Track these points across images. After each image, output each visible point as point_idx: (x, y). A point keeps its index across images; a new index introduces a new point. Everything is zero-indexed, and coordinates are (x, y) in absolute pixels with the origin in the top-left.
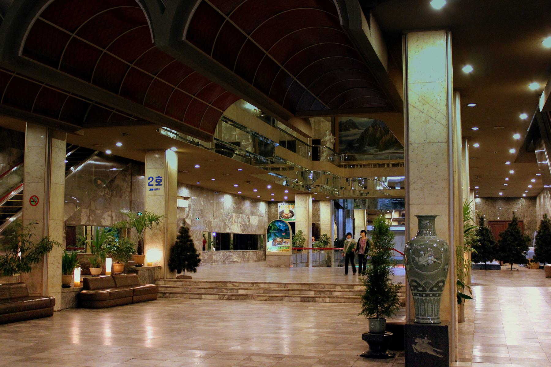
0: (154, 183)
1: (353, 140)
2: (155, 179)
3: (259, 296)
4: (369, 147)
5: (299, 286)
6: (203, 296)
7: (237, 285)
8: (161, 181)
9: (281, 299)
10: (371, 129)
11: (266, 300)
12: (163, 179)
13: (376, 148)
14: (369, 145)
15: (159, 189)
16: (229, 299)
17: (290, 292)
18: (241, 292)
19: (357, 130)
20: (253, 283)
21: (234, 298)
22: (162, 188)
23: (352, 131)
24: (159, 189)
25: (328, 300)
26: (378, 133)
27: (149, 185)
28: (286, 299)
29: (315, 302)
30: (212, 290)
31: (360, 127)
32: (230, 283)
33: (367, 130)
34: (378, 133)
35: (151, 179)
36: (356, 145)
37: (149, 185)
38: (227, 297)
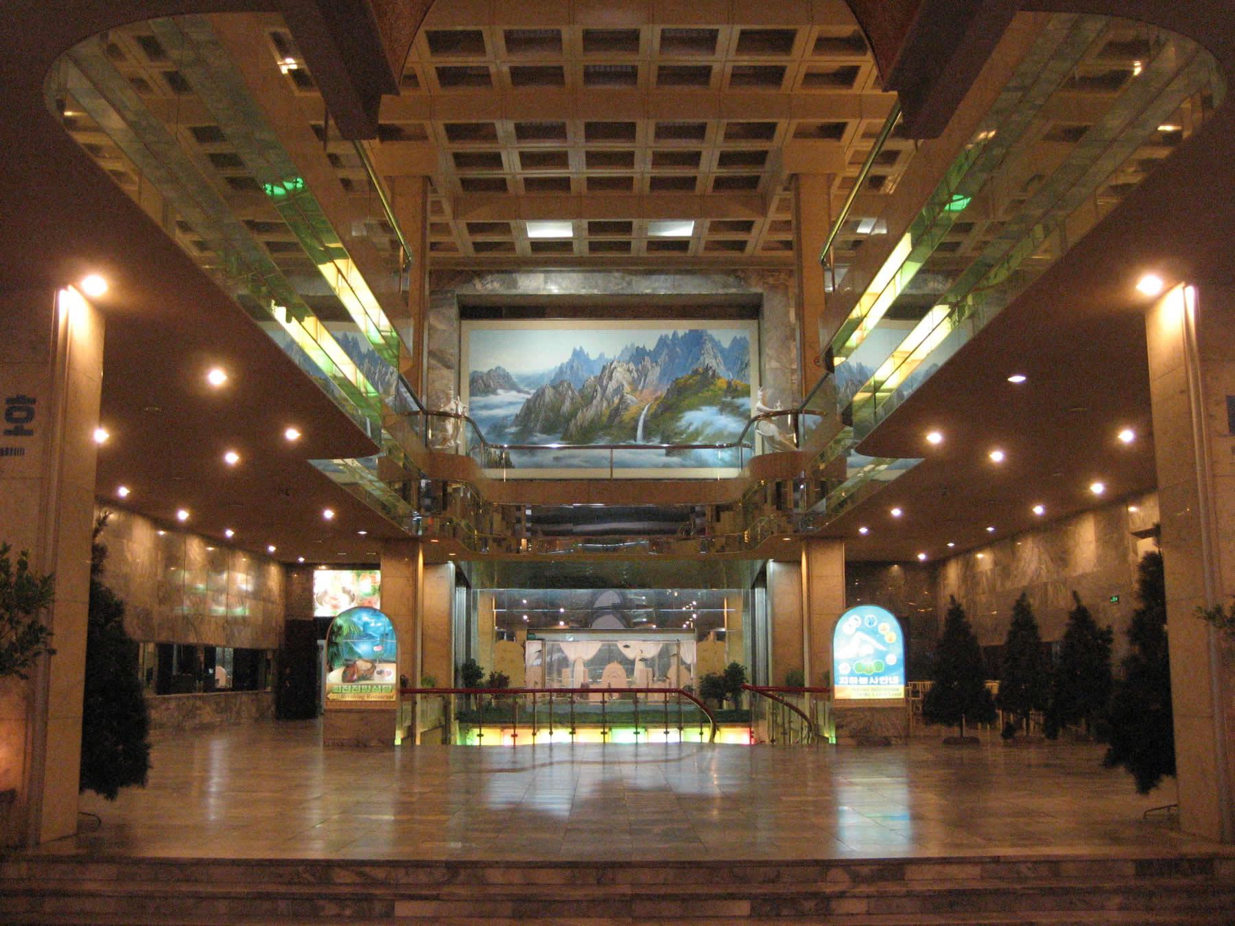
1: (506, 418)
4: (544, 436)
10: (549, 393)
13: (562, 439)
19: (514, 393)
23: (503, 396)
31: (522, 387)
33: (540, 394)
36: (513, 430)
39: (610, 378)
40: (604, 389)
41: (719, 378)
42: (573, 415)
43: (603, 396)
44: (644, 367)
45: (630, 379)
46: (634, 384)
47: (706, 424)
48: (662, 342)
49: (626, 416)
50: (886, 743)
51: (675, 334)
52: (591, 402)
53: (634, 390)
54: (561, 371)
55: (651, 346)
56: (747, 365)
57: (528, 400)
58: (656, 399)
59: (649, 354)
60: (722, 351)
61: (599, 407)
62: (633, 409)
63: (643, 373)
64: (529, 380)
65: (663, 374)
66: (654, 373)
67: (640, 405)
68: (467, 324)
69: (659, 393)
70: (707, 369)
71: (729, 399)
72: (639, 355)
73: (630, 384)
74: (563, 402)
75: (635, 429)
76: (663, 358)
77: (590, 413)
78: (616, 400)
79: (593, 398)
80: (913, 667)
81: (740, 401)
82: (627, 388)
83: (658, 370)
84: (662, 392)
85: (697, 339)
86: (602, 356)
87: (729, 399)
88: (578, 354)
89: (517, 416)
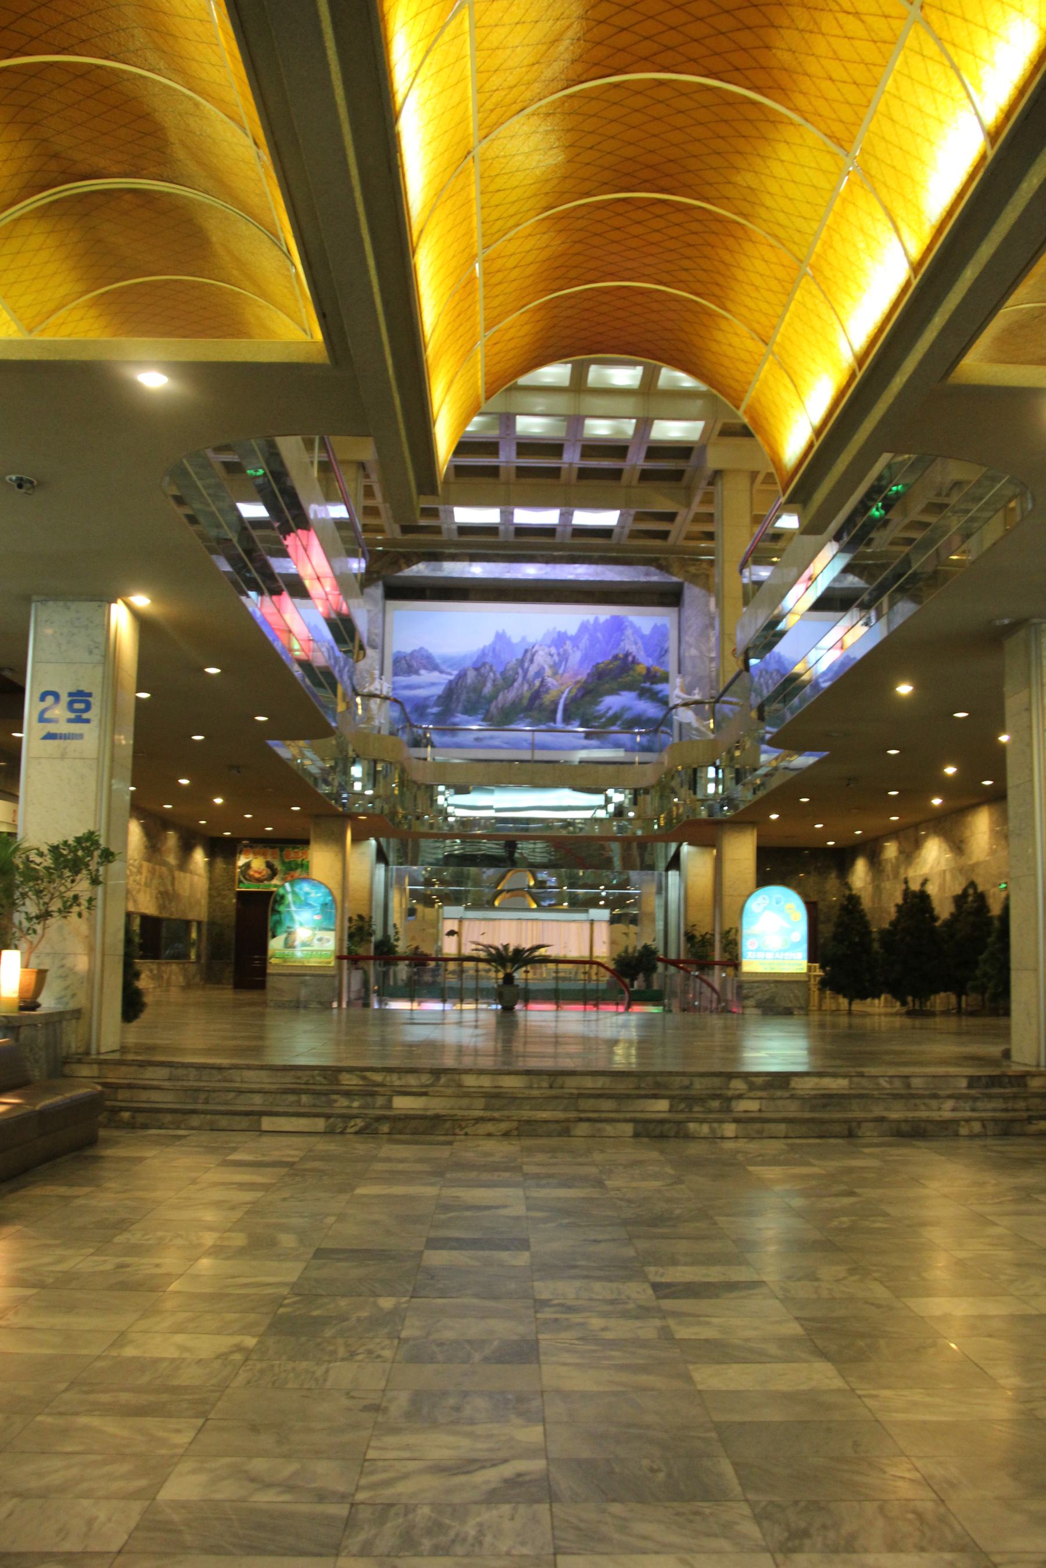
0: (60, 712)
1: (427, 698)
2: (65, 699)
4: (465, 717)
5: (600, 1082)
6: (267, 1123)
7: (378, 1078)
8: (88, 708)
10: (471, 675)
11: (506, 1135)
12: (95, 701)
13: (483, 720)
14: (466, 711)
15: (80, 736)
16: (368, 1131)
17: (583, 1104)
18: (402, 1104)
19: (436, 674)
21: (385, 1128)
23: (426, 676)
24: (80, 736)
26: (489, 685)
27: (42, 719)
28: (583, 1129)
29: (688, 1137)
30: (292, 1098)
31: (444, 667)
32: (351, 1070)
33: (462, 676)
34: (489, 685)
35: (50, 699)
36: (435, 710)
37: (42, 719)
38: (360, 1123)
39: (532, 661)
40: (526, 672)
41: (638, 664)
42: (496, 698)
43: (525, 677)
44: (565, 651)
45: (552, 663)
46: (555, 667)
47: (625, 709)
48: (584, 627)
49: (547, 699)
50: (788, 1012)
51: (596, 620)
52: (512, 685)
53: (555, 674)
54: (483, 653)
56: (666, 651)
57: (450, 682)
58: (577, 683)
59: (571, 638)
60: (642, 637)
61: (520, 690)
63: (564, 657)
65: (585, 658)
66: (575, 657)
67: (561, 688)
68: (391, 604)
69: (579, 678)
71: (648, 685)
72: (560, 639)
73: (551, 667)
74: (484, 685)
75: (554, 711)
76: (584, 642)
77: (511, 695)
78: (537, 683)
79: (514, 680)
81: (658, 687)
82: (548, 672)
84: (582, 677)
85: (617, 626)
86: (524, 639)
87: (648, 685)
88: (500, 637)
89: (439, 697)
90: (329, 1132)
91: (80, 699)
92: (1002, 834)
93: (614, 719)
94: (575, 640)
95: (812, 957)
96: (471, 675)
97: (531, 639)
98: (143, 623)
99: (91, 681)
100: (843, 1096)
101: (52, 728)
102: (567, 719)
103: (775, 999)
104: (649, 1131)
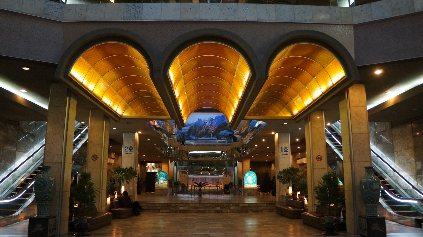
0: (128, 150)
2: (129, 148)
3: (192, 210)
6: (161, 211)
9: (204, 212)
10: (193, 127)
11: (196, 212)
18: (181, 208)
20: (186, 204)
22: (133, 153)
25: (229, 211)
27: (125, 151)
28: (207, 211)
32: (173, 204)
33: (192, 128)
37: (125, 151)
40: (205, 127)
46: (211, 125)
47: (225, 134)
48: (216, 117)
49: (209, 132)
50: (253, 195)
53: (211, 127)
54: (196, 123)
55: (214, 118)
59: (214, 119)
61: (204, 130)
62: (210, 131)
63: (212, 123)
64: (189, 125)
67: (212, 130)
70: (225, 123)
72: (212, 120)
77: (202, 131)
80: (258, 182)
82: (209, 127)
83: (215, 123)
84: (216, 127)
88: (199, 120)
90: (170, 212)
91: (131, 148)
92: (275, 166)
93: (223, 136)
94: (215, 120)
95: (257, 184)
96: (193, 127)
97: (206, 120)
98: (139, 135)
99: (132, 145)
100: (247, 207)
101: (127, 152)
102: (213, 136)
103: (251, 192)
104: (217, 212)
